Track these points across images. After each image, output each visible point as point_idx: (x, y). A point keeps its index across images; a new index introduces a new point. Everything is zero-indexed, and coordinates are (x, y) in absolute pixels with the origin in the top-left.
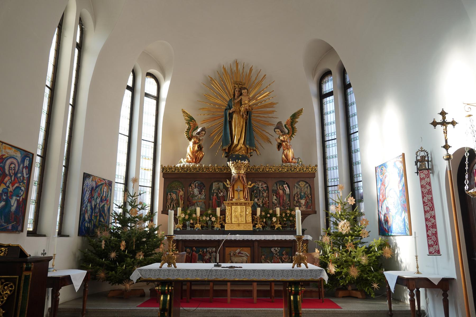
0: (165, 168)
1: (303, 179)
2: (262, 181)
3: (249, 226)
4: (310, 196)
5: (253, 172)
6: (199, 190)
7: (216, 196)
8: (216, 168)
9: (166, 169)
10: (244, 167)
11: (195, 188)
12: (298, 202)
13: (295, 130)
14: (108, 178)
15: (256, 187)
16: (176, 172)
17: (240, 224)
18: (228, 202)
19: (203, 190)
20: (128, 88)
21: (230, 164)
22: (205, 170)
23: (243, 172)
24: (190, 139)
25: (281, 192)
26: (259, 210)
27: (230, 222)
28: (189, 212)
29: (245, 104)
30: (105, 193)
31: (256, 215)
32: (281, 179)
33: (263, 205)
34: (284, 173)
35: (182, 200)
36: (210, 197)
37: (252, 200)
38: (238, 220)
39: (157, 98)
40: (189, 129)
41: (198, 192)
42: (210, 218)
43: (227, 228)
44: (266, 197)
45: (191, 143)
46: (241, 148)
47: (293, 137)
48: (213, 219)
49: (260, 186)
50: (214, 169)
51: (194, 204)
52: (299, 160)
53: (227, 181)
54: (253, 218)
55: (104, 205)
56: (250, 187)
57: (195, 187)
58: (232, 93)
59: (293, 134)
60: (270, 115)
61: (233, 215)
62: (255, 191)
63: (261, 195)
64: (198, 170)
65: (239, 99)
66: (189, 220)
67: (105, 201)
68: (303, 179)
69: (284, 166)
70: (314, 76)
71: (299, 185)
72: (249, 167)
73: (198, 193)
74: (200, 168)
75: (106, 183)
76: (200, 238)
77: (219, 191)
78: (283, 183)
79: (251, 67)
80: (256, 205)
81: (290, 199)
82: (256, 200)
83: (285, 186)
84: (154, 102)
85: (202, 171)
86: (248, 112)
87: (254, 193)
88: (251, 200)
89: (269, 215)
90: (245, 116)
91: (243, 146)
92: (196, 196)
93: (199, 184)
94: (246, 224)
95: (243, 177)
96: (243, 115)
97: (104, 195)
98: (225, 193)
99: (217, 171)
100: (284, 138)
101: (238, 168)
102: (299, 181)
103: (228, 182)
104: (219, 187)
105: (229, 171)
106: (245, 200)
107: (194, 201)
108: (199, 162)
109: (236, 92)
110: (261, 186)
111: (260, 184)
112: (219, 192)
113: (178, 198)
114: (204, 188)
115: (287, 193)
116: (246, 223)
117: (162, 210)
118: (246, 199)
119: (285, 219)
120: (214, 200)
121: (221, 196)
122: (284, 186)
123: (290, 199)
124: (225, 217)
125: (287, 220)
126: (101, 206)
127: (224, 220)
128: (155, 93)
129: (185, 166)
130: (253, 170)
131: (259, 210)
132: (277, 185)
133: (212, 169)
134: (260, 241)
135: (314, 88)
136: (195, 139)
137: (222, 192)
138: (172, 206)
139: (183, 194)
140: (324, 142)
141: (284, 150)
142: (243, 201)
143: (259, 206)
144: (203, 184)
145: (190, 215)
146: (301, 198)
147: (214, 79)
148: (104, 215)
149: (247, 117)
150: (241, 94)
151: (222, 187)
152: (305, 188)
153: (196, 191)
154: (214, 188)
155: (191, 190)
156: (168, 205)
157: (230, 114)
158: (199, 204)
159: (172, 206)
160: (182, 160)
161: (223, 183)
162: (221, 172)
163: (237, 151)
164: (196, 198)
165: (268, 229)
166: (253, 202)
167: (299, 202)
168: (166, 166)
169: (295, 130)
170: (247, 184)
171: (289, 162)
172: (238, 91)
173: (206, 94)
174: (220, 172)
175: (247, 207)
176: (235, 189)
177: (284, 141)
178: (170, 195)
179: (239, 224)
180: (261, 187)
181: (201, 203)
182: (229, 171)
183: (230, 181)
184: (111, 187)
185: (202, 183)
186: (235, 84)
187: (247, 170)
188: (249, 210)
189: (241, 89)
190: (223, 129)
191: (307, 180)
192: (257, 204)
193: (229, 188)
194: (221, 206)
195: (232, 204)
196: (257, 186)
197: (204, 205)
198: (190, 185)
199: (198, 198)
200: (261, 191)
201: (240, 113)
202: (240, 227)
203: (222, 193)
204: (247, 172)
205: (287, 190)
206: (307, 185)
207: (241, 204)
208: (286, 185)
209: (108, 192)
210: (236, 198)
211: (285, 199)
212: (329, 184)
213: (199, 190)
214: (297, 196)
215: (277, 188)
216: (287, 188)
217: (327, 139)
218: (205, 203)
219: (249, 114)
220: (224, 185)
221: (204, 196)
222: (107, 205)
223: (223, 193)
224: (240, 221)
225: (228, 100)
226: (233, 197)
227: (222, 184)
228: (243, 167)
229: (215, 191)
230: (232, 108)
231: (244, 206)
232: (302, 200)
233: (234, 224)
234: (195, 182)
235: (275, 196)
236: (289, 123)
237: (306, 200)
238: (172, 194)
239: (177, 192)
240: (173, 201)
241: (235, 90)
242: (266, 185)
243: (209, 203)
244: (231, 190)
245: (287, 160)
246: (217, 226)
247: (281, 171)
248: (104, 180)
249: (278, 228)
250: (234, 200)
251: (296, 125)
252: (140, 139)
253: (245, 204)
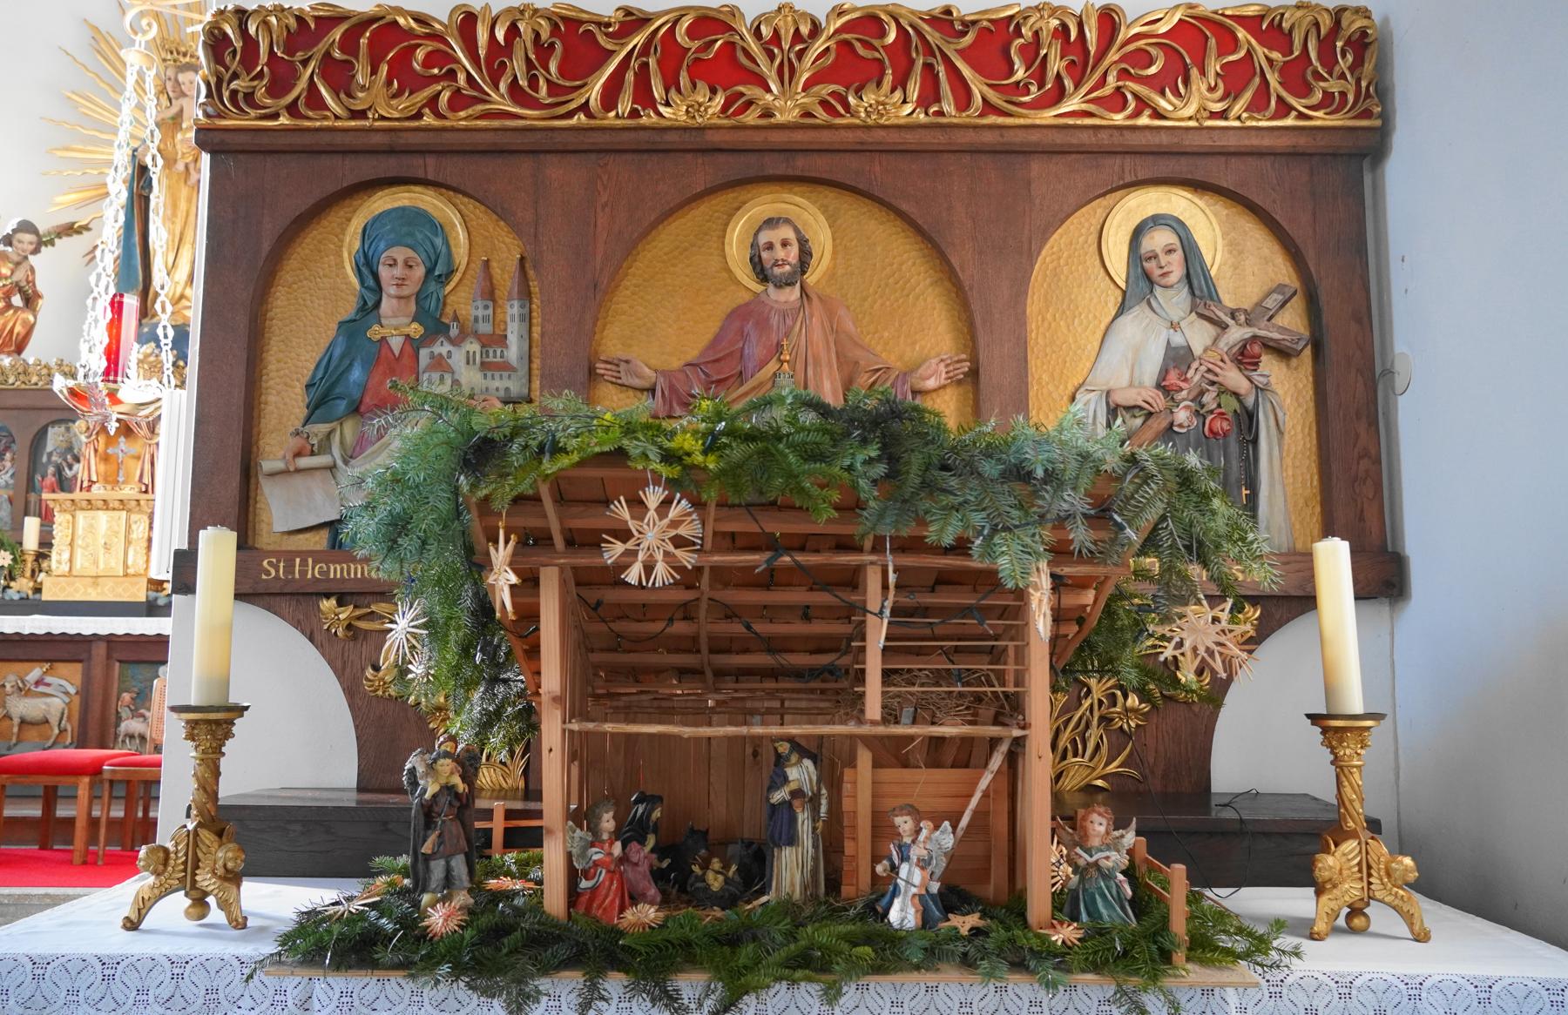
27: (65, 568)
38: (96, 563)
106: (141, 492)
112: (65, 460)
116: (126, 575)
118: (147, 486)
133: (39, 375)
134: (111, 640)
154: (49, 448)
175: (134, 517)
203: (76, 467)
224: (102, 566)
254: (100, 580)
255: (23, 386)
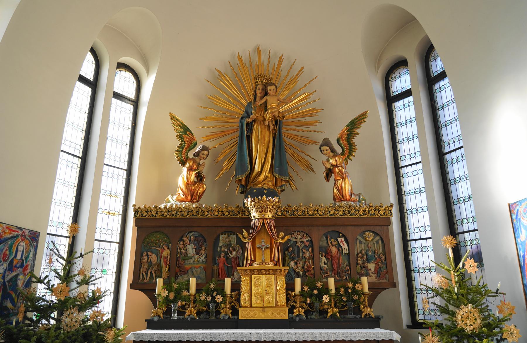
0: (139, 210)
1: (371, 228)
2: (302, 232)
3: (281, 311)
4: (383, 257)
5: (287, 215)
6: (196, 247)
7: (224, 257)
8: (224, 210)
9: (141, 211)
10: (272, 207)
11: (189, 244)
12: (364, 267)
13: (354, 147)
14: (29, 225)
15: (292, 242)
16: (158, 216)
17: (265, 307)
18: (244, 268)
19: (203, 248)
20: (82, 79)
21: (249, 202)
22: (206, 214)
23: (270, 217)
24: (183, 163)
25: (334, 250)
26: (298, 282)
27: (248, 304)
28: (175, 286)
29: (273, 108)
30: (19, 254)
31: (293, 290)
32: (333, 229)
33: (305, 272)
34: (338, 217)
35: (166, 265)
36: (214, 259)
37: (285, 264)
38: (263, 300)
39: (136, 103)
40: (181, 147)
41: (194, 250)
42: (213, 298)
43: (243, 315)
44: (309, 259)
45: (185, 170)
46: (266, 178)
47: (351, 160)
48: (219, 299)
49: (299, 240)
50: (222, 212)
51: (188, 271)
52: (361, 197)
53: (243, 232)
54: (288, 296)
55: (17, 275)
56: (282, 241)
57: (190, 241)
58: (251, 94)
59: (350, 154)
60: (311, 128)
61: (253, 291)
62: (291, 249)
63: (301, 255)
64: (194, 213)
65: (263, 101)
66: (175, 301)
67: (19, 268)
68: (371, 228)
69: (338, 206)
70: (377, 68)
71: (364, 238)
72: (279, 207)
73: (195, 253)
74: (197, 210)
75: (23, 236)
76: (191, 338)
77: (230, 248)
78: (338, 234)
79: (281, 55)
80: (293, 273)
81: (349, 263)
82: (292, 263)
83: (341, 240)
84: (130, 108)
85: (201, 216)
86: (277, 122)
87: (289, 252)
88: (284, 265)
89: (316, 292)
90: (272, 127)
91: (269, 175)
92: (191, 258)
93: (195, 237)
94: (276, 308)
95: (269, 225)
96: (269, 126)
97: (19, 257)
98: (240, 253)
99: (226, 214)
100: (336, 161)
101: (261, 209)
102: (364, 232)
103: (245, 233)
104: (230, 241)
105: (246, 214)
106: (275, 265)
107: (187, 266)
108: (198, 201)
109: (257, 90)
110: (300, 239)
111: (299, 237)
113: (160, 260)
114: (205, 244)
115: (344, 252)
116: (277, 306)
117: (132, 283)
118: (276, 262)
119: (344, 299)
120: (221, 265)
121: (233, 257)
122: (339, 239)
123: (349, 263)
124: (239, 295)
125: (347, 301)
126: (7, 279)
127: (239, 300)
128: (131, 94)
129: (174, 207)
130: (287, 214)
131: (298, 282)
132: (327, 238)
133: (218, 212)
135: (378, 88)
136: (191, 163)
137: (235, 250)
138: (149, 275)
139: (169, 254)
140: (397, 168)
141: (336, 180)
142: (270, 266)
143: (298, 275)
144: (204, 238)
145: (178, 292)
146: (369, 261)
147: (224, 74)
148: (14, 295)
149: (275, 130)
150: (266, 94)
151: (234, 242)
152: (374, 243)
153: (191, 249)
154: (220, 245)
155: (182, 246)
156: (143, 274)
157: (248, 124)
158: (196, 271)
159: (149, 275)
160: (169, 197)
161: (237, 236)
162: (234, 217)
163: (259, 183)
164: (191, 261)
165: (315, 316)
166: (288, 268)
167: (366, 267)
168: (142, 207)
169: (354, 147)
170: (278, 237)
171: (346, 200)
172: (261, 89)
173: (212, 96)
174: (231, 217)
176: (257, 245)
177: (337, 166)
178: (147, 255)
179: (263, 309)
180: (300, 242)
181: (199, 270)
182: (246, 214)
183: (248, 231)
184: (37, 242)
185: (201, 235)
186: (256, 79)
187: (276, 214)
188: (282, 282)
189: (265, 86)
190: (237, 149)
191: (377, 229)
192: (295, 271)
193: (247, 244)
194: (233, 275)
195: (252, 272)
196: (294, 240)
197: (204, 273)
198: (181, 239)
199: (194, 261)
200: (301, 248)
201: (264, 123)
202: (266, 314)
204: (276, 216)
205: (345, 247)
206: (378, 238)
207: (267, 272)
208: (343, 239)
209: (28, 252)
210: (258, 260)
211: (341, 262)
212: (411, 236)
213: (196, 247)
214: (362, 257)
215: (327, 242)
216: (344, 243)
217: (402, 163)
218: (205, 269)
219: (278, 125)
220: (238, 238)
221: (204, 257)
222: (25, 275)
223: (237, 252)
224: (265, 302)
225: (245, 104)
226: (253, 259)
227: (234, 237)
228: (271, 207)
229: (223, 249)
230: (252, 114)
231: (273, 276)
232: (370, 263)
233: (255, 308)
234: (189, 232)
235: (325, 256)
236: (345, 136)
237: (377, 264)
238: (150, 254)
239: (158, 250)
240: (151, 265)
241: (256, 88)
242: (309, 238)
243: (213, 270)
244: (250, 246)
245: (340, 197)
246: (226, 312)
247: (334, 214)
248: (21, 229)
249: (333, 316)
250: (255, 266)
251: (356, 140)
252: (101, 163)
253: (275, 272)
254: (266, 309)
255: (211, 217)
